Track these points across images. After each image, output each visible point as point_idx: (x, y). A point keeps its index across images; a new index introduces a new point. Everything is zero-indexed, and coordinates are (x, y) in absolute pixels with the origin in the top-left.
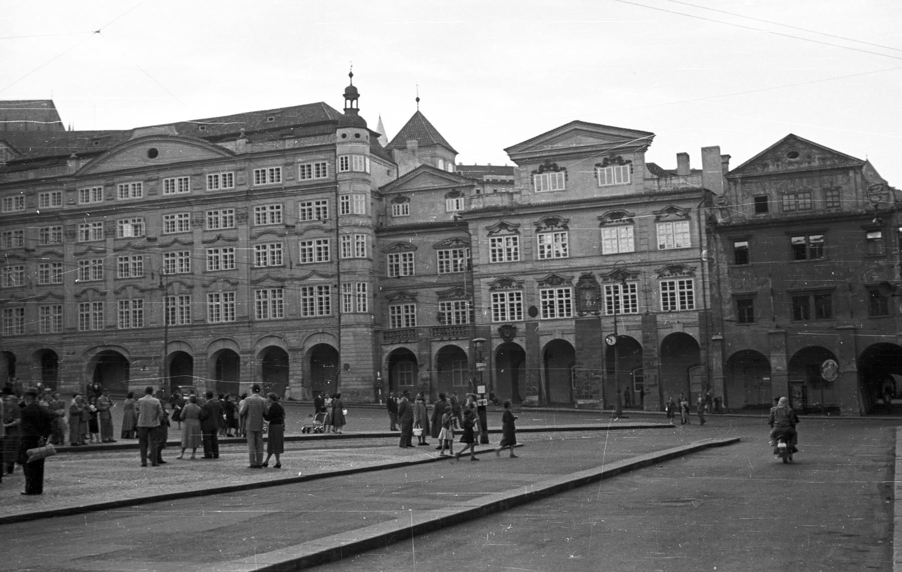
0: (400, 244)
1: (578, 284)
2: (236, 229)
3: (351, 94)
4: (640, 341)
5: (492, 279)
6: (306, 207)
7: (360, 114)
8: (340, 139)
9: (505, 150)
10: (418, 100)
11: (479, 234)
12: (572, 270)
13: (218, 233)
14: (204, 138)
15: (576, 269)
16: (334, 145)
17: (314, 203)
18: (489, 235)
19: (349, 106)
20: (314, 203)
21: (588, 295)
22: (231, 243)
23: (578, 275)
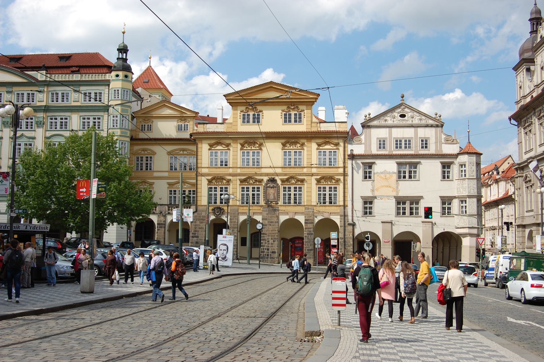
0: (144, 150)
1: (267, 184)
2: (35, 131)
3: (123, 50)
4: (303, 222)
5: (210, 178)
7: (128, 62)
9: (224, 95)
11: (204, 148)
12: (261, 175)
13: (22, 132)
15: (267, 175)
17: (91, 118)
18: (209, 149)
19: (120, 57)
21: (271, 191)
22: (31, 140)
23: (265, 179)
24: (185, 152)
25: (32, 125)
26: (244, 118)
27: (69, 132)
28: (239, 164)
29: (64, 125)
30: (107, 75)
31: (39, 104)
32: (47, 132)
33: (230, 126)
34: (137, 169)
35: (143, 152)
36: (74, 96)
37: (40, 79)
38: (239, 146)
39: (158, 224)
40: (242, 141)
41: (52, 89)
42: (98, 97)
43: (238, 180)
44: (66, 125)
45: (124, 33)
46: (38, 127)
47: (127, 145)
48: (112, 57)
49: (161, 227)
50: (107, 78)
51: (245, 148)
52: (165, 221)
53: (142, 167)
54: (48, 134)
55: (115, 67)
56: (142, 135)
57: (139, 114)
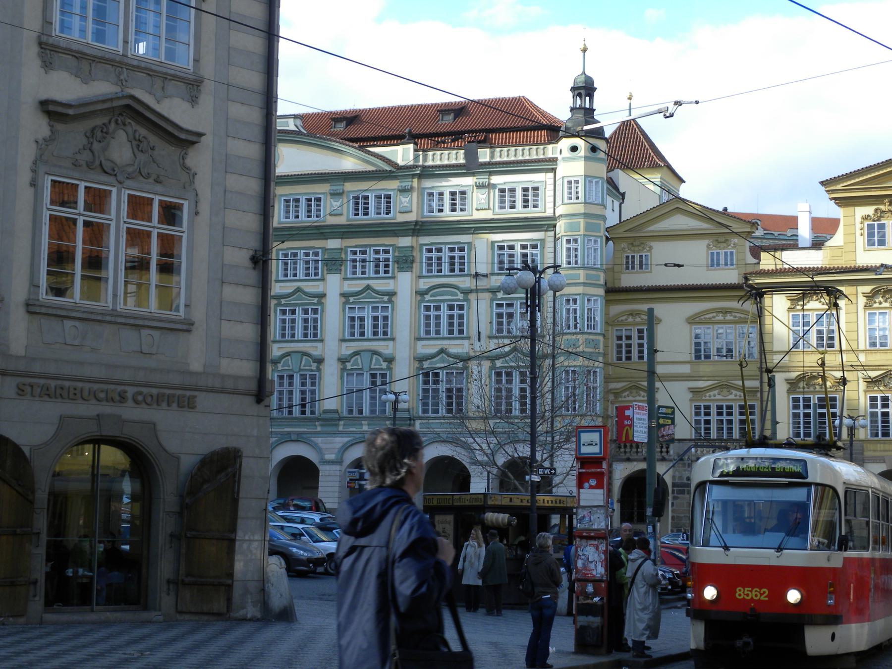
2: (393, 278)
3: (585, 89)
6: (457, 254)
8: (567, 153)
9: (822, 183)
10: (697, 102)
13: (366, 282)
14: (345, 139)
16: (554, 160)
18: (790, 309)
20: (445, 249)
24: (729, 317)
25: (387, 266)
26: (871, 235)
27: (468, 279)
28: (863, 344)
29: (458, 265)
30: (550, 147)
31: (401, 218)
32: (422, 281)
33: (838, 253)
34: (620, 359)
35: (630, 319)
36: (478, 199)
37: (401, 162)
38: (862, 301)
39: (674, 485)
40: (868, 289)
41: (428, 183)
42: (530, 194)
43: (861, 381)
44: (462, 264)
45: (584, 50)
46: (401, 269)
47: (598, 306)
48: (558, 106)
49: (682, 492)
50: (550, 155)
51: (877, 305)
52: (688, 479)
53: (629, 352)
54: (424, 284)
55: (567, 129)
56: (629, 280)
57: (620, 232)
